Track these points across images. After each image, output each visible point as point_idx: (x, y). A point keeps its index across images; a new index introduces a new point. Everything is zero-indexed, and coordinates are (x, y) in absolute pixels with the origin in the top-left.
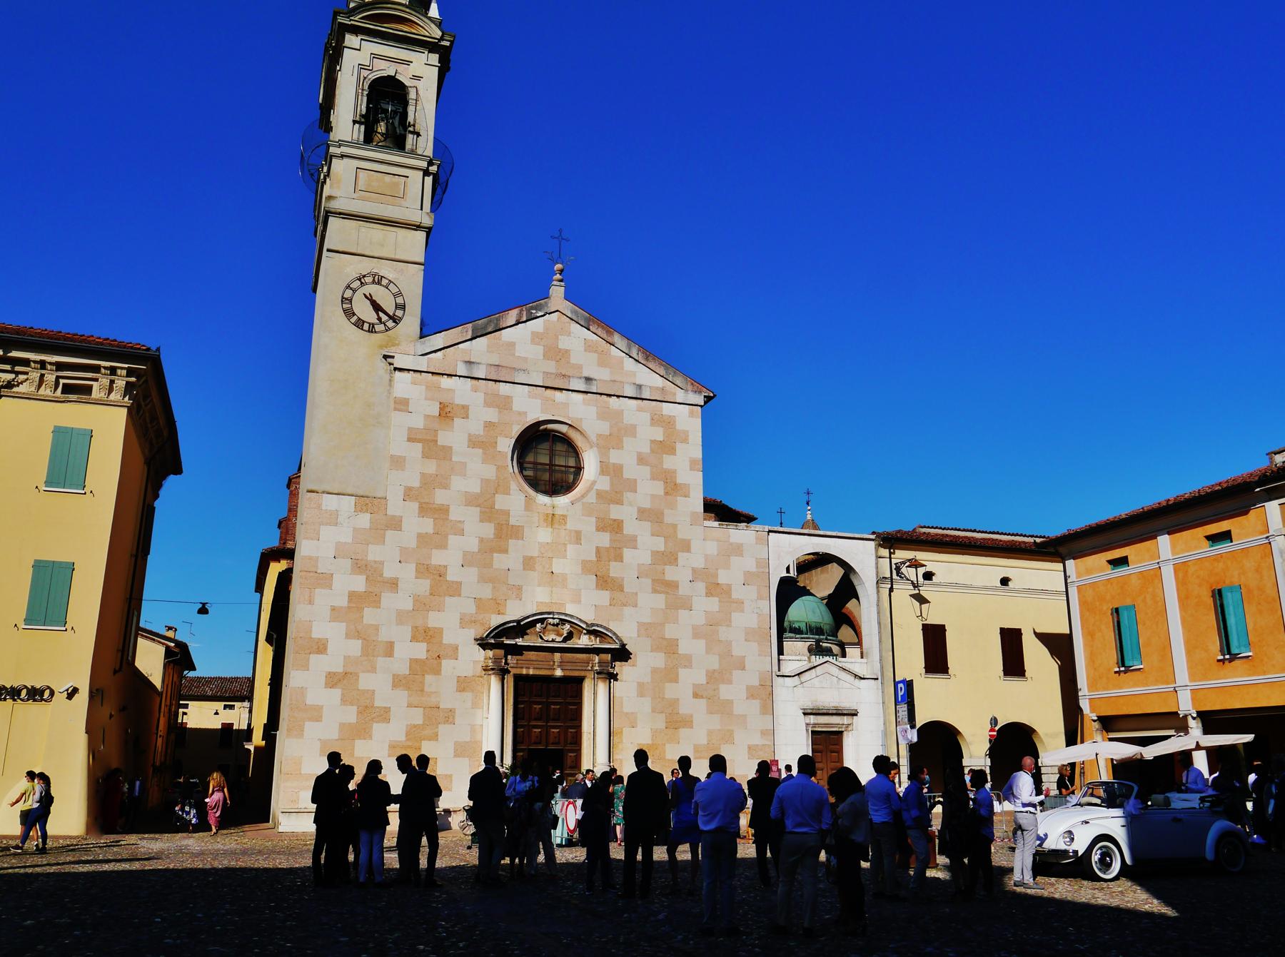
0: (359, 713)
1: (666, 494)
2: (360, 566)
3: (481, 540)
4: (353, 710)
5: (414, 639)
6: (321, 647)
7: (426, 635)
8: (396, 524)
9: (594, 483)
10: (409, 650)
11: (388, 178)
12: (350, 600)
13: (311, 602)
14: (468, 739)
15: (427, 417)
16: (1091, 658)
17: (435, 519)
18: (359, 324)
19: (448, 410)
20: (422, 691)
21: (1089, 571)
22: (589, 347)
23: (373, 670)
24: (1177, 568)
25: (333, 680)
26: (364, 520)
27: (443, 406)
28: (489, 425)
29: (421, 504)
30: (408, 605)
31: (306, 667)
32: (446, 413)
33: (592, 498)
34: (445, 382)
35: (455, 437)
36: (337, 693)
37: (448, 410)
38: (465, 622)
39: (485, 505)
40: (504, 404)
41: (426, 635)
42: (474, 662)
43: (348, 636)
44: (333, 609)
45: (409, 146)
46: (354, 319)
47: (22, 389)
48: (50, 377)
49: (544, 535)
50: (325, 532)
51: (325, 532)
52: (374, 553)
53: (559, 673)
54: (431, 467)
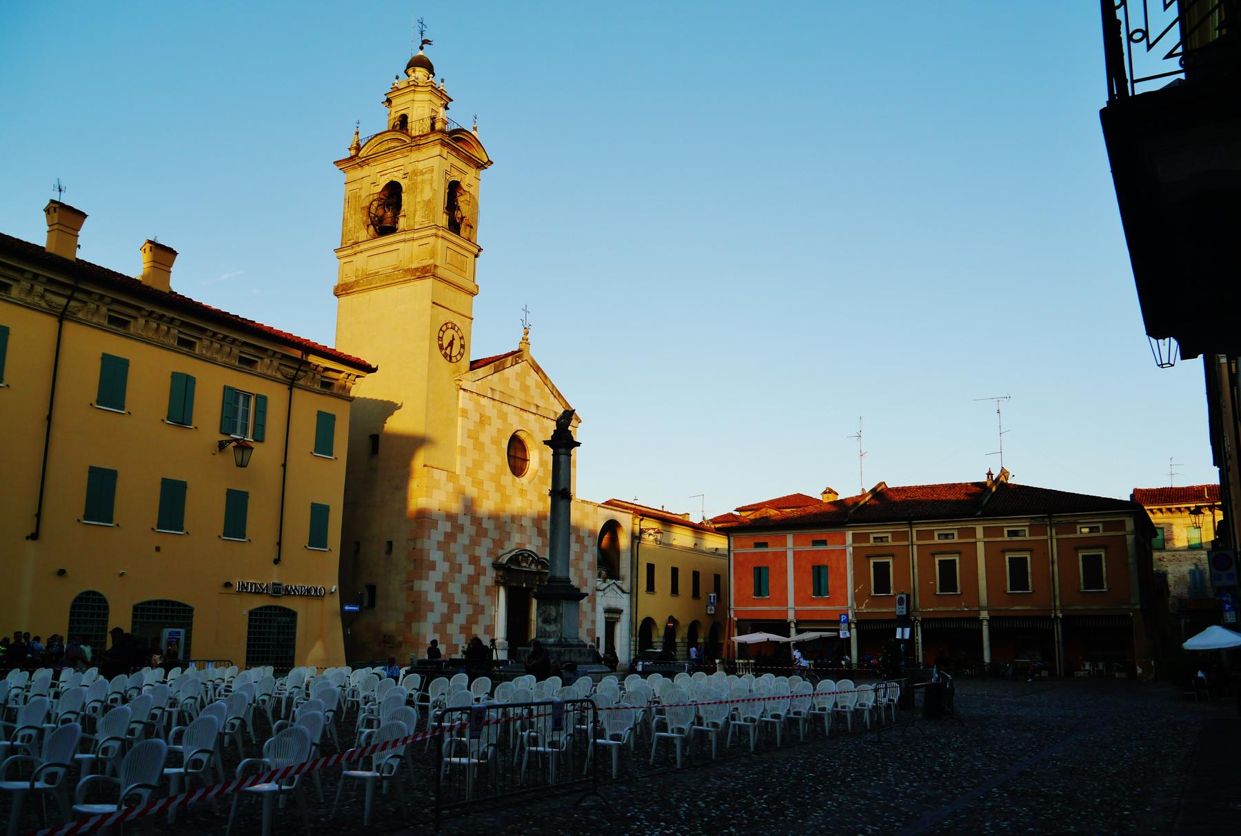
4: (446, 605)
5: (470, 563)
7: (474, 560)
10: (468, 570)
16: (738, 591)
21: (742, 547)
22: (537, 386)
23: (453, 581)
24: (795, 553)
25: (440, 587)
27: (481, 416)
28: (499, 430)
30: (467, 542)
32: (483, 421)
33: (536, 481)
34: (482, 399)
35: (485, 437)
38: (490, 553)
39: (496, 479)
40: (503, 416)
41: (474, 560)
45: (462, 233)
47: (301, 382)
48: (276, 363)
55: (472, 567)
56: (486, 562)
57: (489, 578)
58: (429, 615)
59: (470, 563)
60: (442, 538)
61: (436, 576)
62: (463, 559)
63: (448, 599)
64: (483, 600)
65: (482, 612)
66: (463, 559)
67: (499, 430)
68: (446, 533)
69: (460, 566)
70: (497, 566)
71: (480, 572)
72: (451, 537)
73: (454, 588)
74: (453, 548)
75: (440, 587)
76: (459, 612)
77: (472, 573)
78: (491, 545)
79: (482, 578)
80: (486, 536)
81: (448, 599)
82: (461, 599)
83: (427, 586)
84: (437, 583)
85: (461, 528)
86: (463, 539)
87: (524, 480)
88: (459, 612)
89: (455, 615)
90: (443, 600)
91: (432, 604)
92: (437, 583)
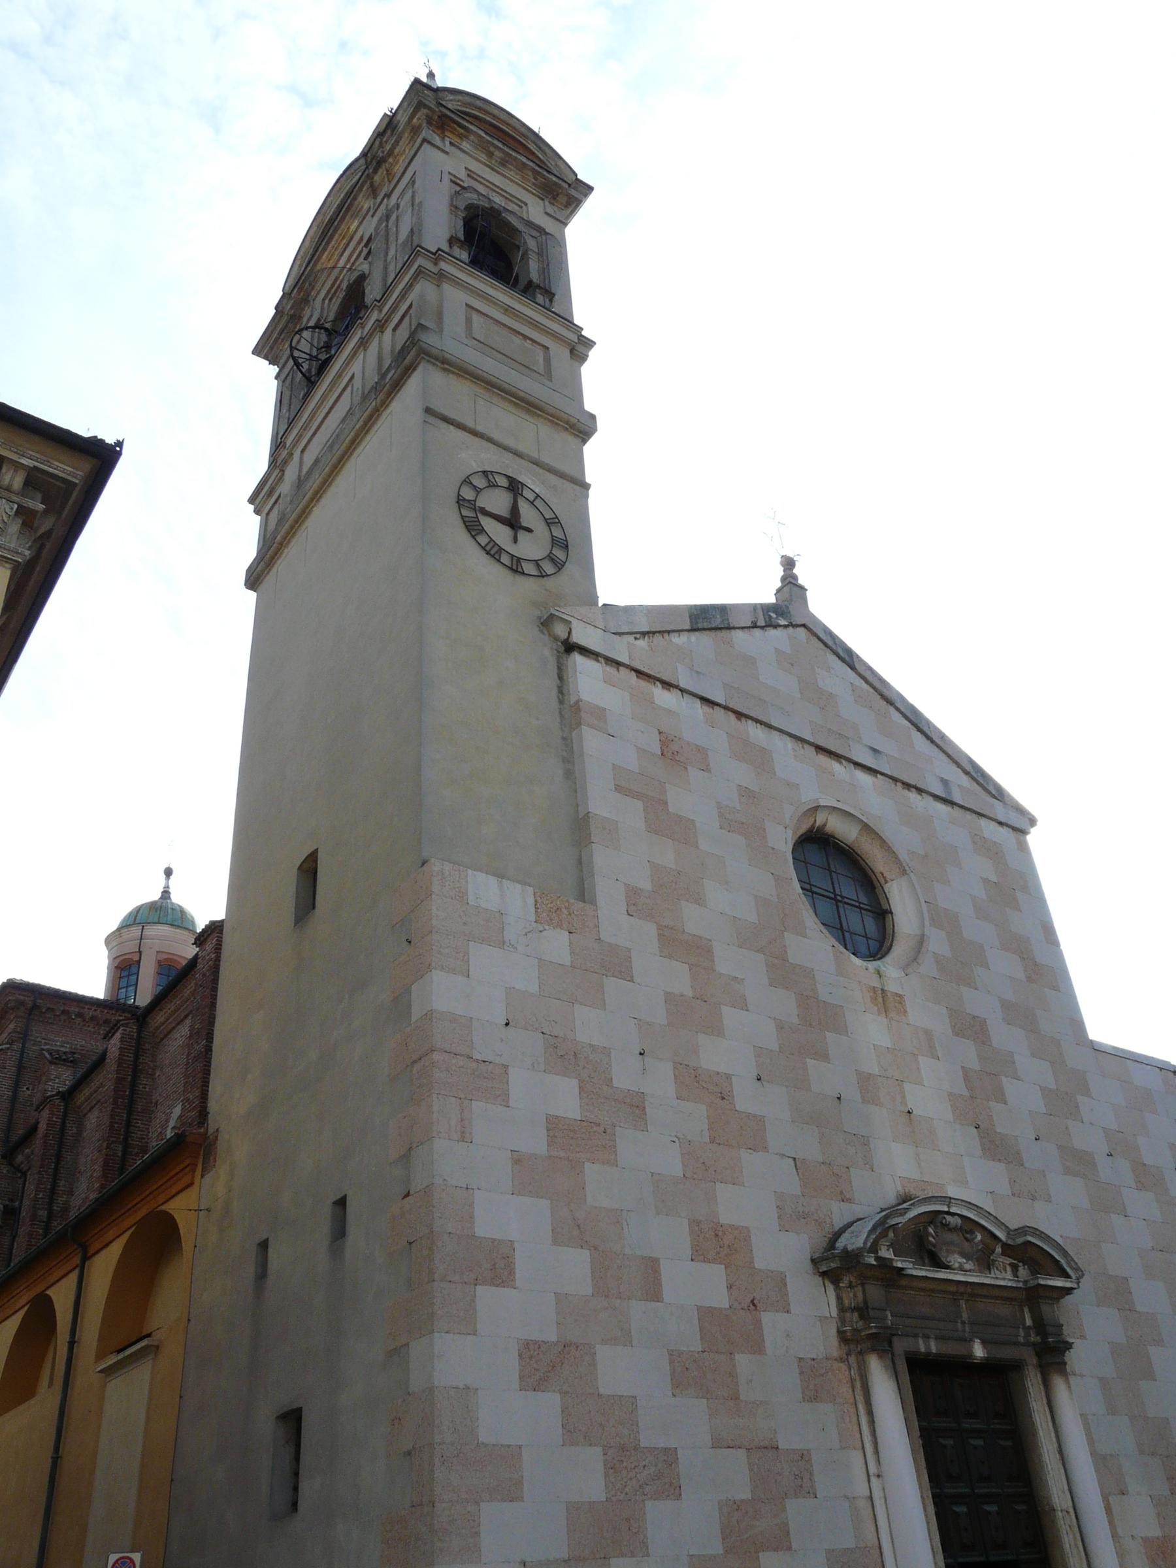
0: (611, 1468)
1: (1029, 979)
2: (563, 1055)
3: (780, 1026)
4: (593, 1457)
5: (699, 1254)
6: (498, 1267)
7: (718, 1243)
8: (618, 964)
9: (921, 941)
11: (517, 340)
12: (551, 1141)
13: (464, 1137)
14: (850, 1543)
15: (641, 751)
17: (691, 966)
18: (493, 552)
19: (674, 747)
20: (736, 1398)
23: (624, 1338)
25: (542, 1365)
26: (557, 945)
27: (666, 741)
28: (745, 793)
29: (660, 928)
30: (671, 1164)
31: (468, 1324)
32: (671, 751)
36: (550, 1402)
37: (674, 747)
38: (790, 1217)
41: (718, 1243)
42: (822, 1319)
43: (557, 1239)
44: (518, 1159)
46: (483, 540)
49: (872, 1031)
50: (482, 957)
51: (482, 957)
52: (588, 1027)
53: (979, 1351)
54: (667, 855)
55: (716, 1274)
56: (785, 1252)
57: (808, 1318)
58: (492, 1513)
59: (699, 1254)
60: (535, 1142)
61: (511, 1316)
62: (664, 1237)
63: (599, 1423)
64: (803, 1426)
65: (803, 1485)
66: (664, 1237)
67: (745, 793)
68: (554, 1125)
69: (651, 1266)
70: (835, 1264)
71: (756, 1297)
72: (576, 1142)
73: (627, 1371)
74: (601, 1187)
75: (542, 1365)
76: (672, 1489)
77: (720, 1299)
78: (792, 1185)
79: (771, 1321)
80: (759, 1144)
81: (599, 1423)
82: (677, 1423)
83: (474, 1362)
84: (529, 1350)
85: (635, 1107)
86: (652, 1152)
87: (890, 968)
88: (672, 1489)
89: (656, 1512)
90: (574, 1432)
91: (510, 1456)
92: (529, 1350)
